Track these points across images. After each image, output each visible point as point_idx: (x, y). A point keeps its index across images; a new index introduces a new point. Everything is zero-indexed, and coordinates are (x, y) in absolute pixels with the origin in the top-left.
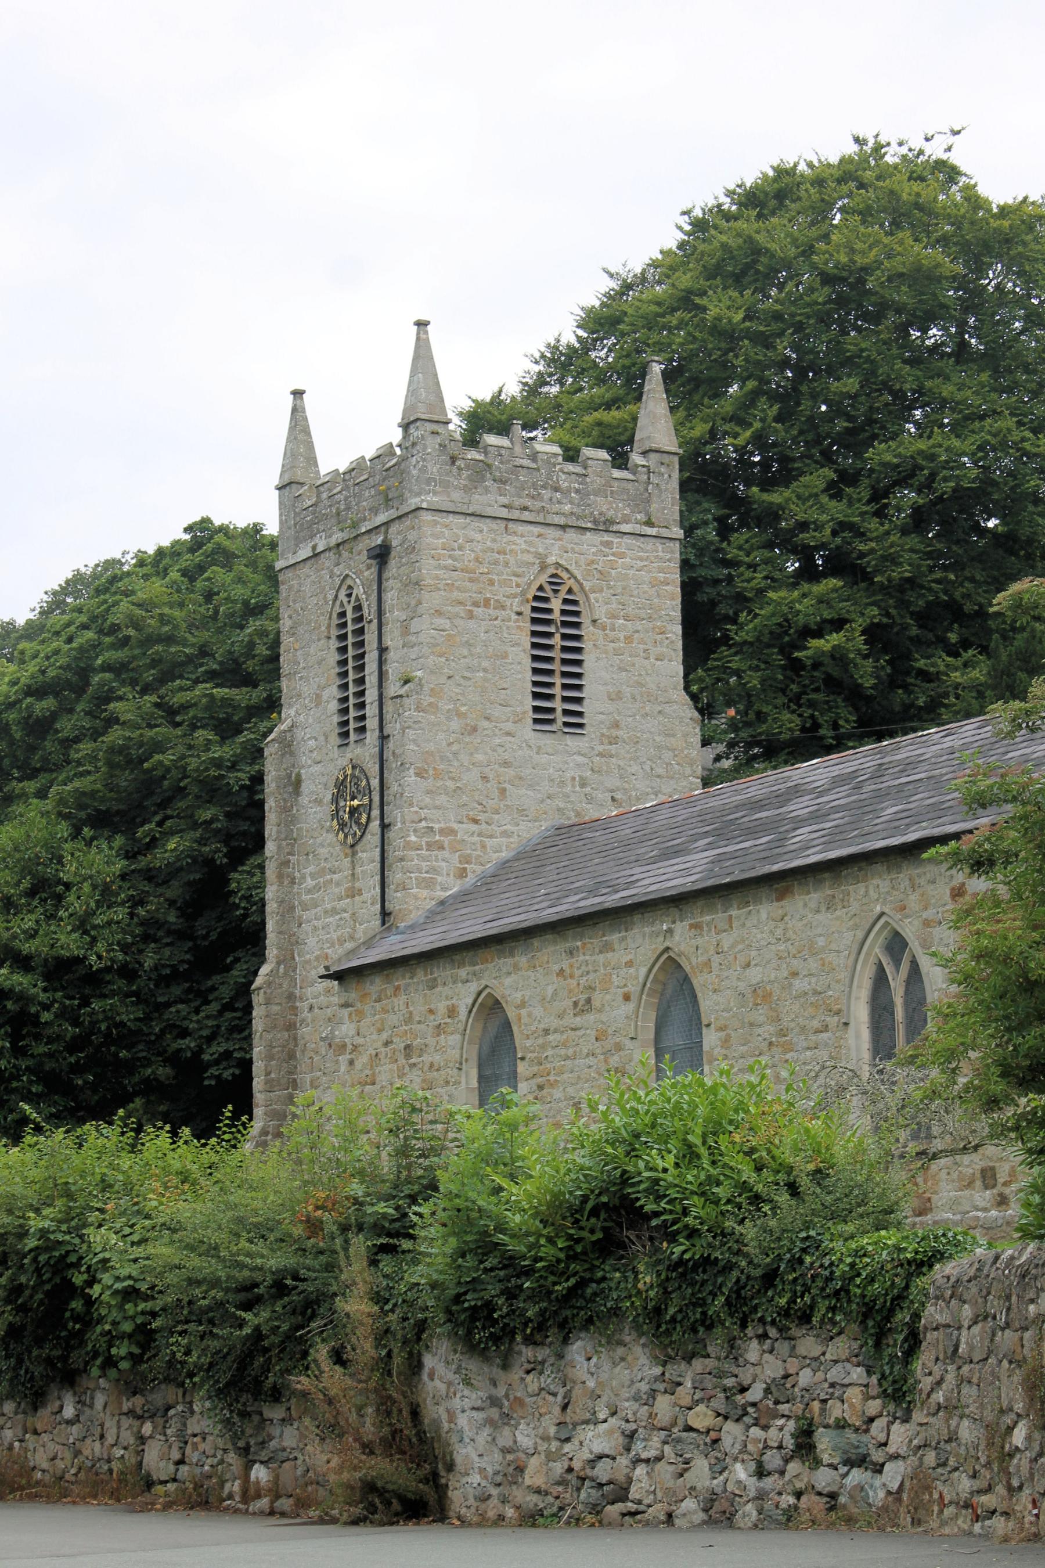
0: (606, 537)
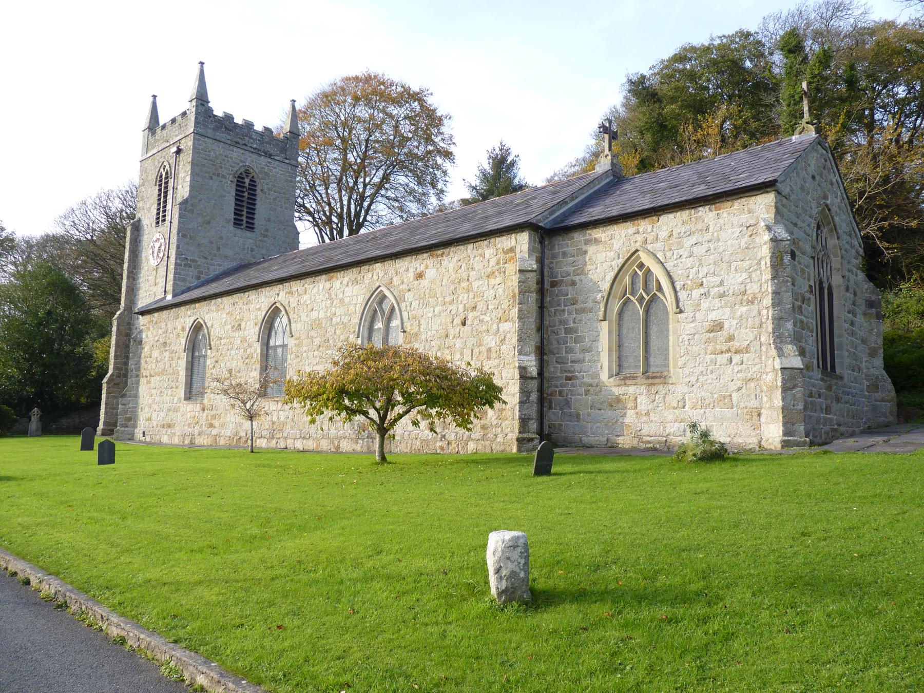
0: (269, 160)
